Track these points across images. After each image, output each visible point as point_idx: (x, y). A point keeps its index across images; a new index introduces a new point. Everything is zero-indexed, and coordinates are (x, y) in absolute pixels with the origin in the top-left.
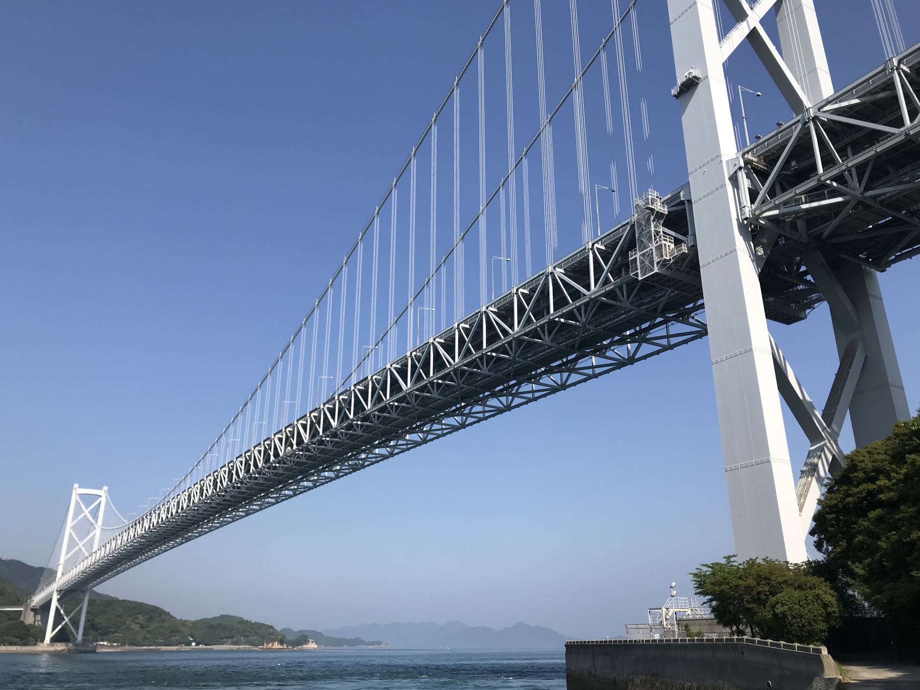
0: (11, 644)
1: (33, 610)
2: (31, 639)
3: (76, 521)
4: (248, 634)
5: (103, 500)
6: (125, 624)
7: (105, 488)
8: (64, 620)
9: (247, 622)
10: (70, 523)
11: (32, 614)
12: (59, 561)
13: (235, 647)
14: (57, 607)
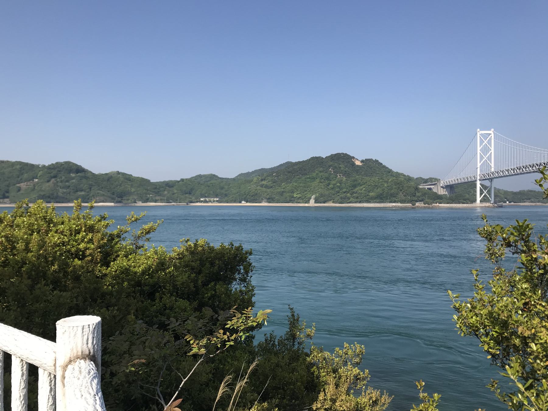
0: (463, 203)
1: (442, 187)
2: (468, 201)
3: (482, 146)
4: (538, 197)
5: (493, 135)
6: (471, 192)
7: (493, 130)
8: (484, 192)
9: (535, 191)
10: (479, 148)
11: (442, 189)
12: (477, 166)
13: (534, 204)
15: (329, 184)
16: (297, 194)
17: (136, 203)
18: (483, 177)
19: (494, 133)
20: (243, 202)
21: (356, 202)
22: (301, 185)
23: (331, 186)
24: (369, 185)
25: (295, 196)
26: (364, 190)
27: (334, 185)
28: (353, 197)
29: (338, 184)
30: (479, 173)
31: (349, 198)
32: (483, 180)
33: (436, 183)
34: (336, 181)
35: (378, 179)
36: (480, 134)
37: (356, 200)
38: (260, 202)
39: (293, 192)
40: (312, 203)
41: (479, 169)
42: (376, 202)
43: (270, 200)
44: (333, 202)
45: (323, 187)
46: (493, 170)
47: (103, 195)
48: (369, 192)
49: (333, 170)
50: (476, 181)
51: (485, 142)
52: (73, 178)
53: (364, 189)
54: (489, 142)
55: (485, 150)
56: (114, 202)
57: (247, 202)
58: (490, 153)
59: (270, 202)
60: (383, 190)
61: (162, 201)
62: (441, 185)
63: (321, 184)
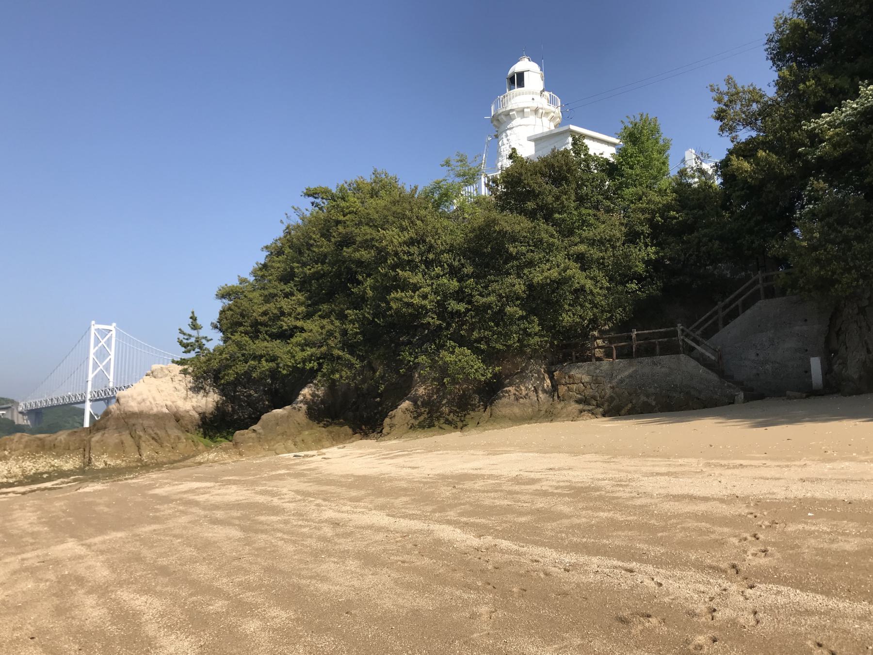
1: (21, 413)
3: (97, 348)
5: (114, 333)
7: (114, 324)
10: (92, 351)
11: (20, 416)
14: (90, 412)
18: (96, 396)
19: (117, 330)
30: (89, 389)
32: (96, 400)
33: (10, 405)
36: (96, 330)
41: (90, 384)
46: (111, 385)
50: (84, 402)
51: (103, 342)
54: (109, 343)
55: (102, 354)
58: (108, 359)
62: (20, 409)
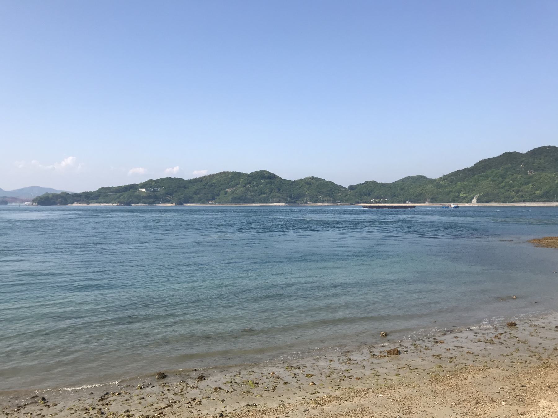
15: (502, 182)
16: (464, 194)
17: (307, 203)
20: (407, 202)
21: (520, 202)
22: (472, 183)
23: (503, 184)
24: (541, 183)
25: (461, 196)
26: (532, 188)
27: (506, 183)
28: (517, 197)
29: (511, 182)
31: (513, 197)
34: (511, 178)
35: (556, 174)
37: (521, 199)
38: (424, 203)
39: (459, 192)
40: (474, 203)
42: (541, 201)
43: (433, 200)
44: (496, 202)
45: (492, 185)
47: (279, 197)
48: (537, 190)
49: (524, 166)
52: (262, 184)
53: (531, 186)
56: (285, 203)
57: (412, 202)
59: (432, 203)
60: (550, 187)
61: (328, 201)
63: (491, 182)
